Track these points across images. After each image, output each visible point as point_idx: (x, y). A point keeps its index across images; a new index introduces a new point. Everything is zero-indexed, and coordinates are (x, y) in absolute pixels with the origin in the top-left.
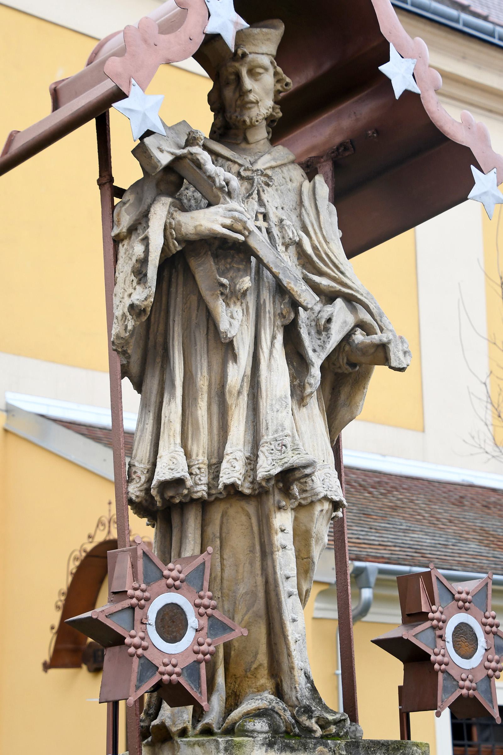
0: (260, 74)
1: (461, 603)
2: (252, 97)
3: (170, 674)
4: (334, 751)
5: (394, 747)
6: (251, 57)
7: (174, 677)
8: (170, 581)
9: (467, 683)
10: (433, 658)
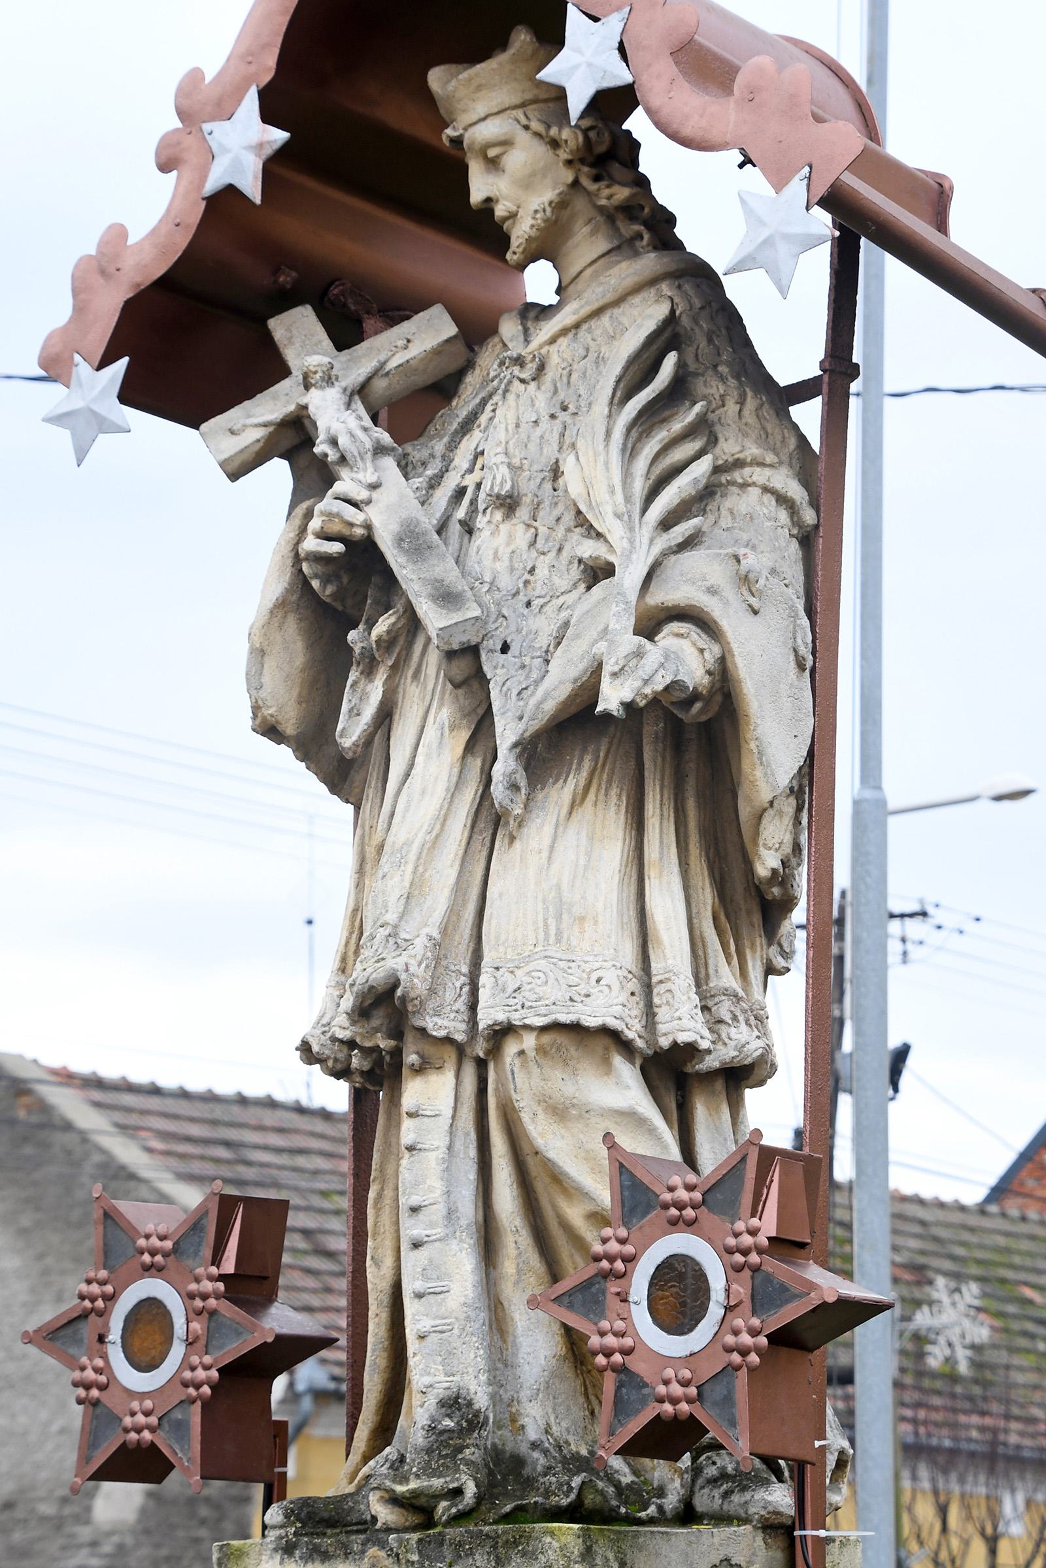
0: (498, 157)
1: (674, 1212)
2: (500, 211)
3: (139, 1431)
4: (397, 1555)
5: (507, 1541)
6: (467, 136)
7: (147, 1435)
8: (146, 1258)
9: (676, 1390)
10: (595, 1341)
